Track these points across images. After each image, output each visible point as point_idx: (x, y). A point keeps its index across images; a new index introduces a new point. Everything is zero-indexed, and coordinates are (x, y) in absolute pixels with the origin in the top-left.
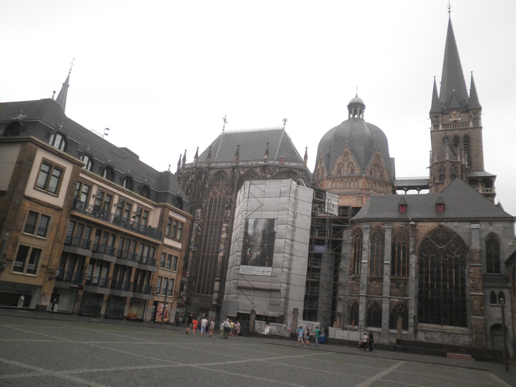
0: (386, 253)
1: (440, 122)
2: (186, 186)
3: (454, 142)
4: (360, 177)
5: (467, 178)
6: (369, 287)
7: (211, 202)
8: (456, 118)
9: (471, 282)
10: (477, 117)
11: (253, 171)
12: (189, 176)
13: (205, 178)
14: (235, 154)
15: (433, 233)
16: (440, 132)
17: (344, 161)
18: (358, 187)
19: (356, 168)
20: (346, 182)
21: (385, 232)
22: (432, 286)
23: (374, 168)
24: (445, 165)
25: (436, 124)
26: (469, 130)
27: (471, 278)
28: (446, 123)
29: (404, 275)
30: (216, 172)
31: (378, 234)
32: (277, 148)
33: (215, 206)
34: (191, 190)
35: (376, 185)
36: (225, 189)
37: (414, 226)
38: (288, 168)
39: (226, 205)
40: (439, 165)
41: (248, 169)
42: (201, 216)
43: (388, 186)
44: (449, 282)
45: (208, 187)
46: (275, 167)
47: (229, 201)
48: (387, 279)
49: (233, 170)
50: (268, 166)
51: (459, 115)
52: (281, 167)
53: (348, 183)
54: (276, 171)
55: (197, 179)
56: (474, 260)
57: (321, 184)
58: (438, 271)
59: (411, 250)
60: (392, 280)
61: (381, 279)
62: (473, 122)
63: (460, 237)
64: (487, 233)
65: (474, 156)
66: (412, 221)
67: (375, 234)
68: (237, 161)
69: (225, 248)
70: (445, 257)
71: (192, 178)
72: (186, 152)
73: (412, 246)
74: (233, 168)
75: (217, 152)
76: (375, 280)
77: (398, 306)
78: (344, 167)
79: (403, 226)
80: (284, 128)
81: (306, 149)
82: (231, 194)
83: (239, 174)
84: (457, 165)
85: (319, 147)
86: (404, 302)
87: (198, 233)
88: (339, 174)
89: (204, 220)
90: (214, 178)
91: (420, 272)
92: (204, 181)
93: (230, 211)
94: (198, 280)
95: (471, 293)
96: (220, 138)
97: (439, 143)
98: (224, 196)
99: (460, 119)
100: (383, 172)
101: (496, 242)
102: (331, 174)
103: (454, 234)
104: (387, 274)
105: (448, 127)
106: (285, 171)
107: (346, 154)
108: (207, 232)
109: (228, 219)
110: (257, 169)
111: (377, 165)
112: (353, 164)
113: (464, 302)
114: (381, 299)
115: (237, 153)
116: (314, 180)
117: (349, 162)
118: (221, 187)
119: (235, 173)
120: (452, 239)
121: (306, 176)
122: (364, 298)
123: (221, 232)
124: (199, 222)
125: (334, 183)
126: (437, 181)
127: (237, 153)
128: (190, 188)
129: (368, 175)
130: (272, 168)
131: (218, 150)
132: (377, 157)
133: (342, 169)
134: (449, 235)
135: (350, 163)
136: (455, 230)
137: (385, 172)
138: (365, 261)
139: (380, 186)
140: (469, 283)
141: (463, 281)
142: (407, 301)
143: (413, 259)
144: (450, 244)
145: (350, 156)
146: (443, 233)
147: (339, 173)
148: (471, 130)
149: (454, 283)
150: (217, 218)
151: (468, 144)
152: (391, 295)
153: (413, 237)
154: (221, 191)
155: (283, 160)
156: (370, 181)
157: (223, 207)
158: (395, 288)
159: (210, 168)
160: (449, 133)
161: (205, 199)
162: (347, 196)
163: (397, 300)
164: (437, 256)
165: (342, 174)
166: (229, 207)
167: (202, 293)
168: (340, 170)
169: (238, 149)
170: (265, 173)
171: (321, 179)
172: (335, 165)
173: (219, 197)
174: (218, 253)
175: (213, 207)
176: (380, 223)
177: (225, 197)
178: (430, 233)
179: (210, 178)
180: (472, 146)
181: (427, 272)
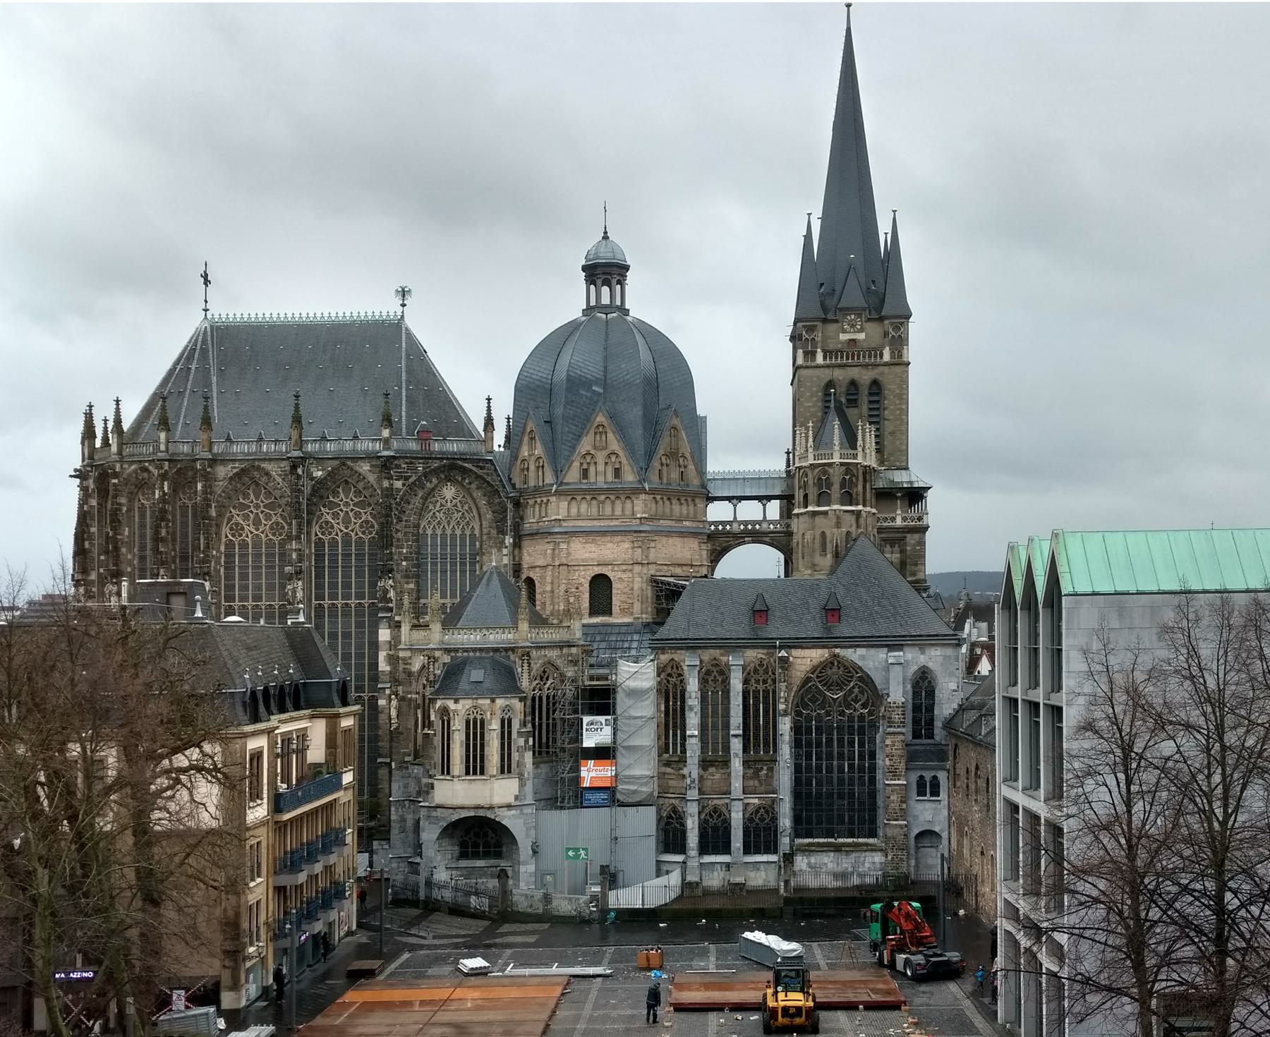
0: (732, 713)
1: (819, 345)
2: (136, 509)
5: (874, 491)
6: (701, 778)
7: (229, 556)
9: (888, 763)
12: (143, 479)
13: (205, 492)
14: (290, 421)
15: (820, 669)
16: (817, 371)
18: (633, 515)
20: (603, 502)
21: (730, 670)
22: (819, 769)
24: (831, 471)
26: (881, 368)
27: (887, 756)
28: (831, 347)
29: (766, 752)
30: (235, 471)
31: (715, 673)
32: (400, 388)
34: (167, 526)
35: (671, 503)
36: (268, 517)
37: (784, 661)
38: (447, 459)
39: (288, 569)
40: (817, 470)
41: (336, 463)
43: (697, 501)
44: (849, 760)
46: (411, 458)
47: (294, 556)
48: (737, 765)
51: (861, 325)
53: (608, 502)
55: (174, 491)
56: (894, 722)
57: (539, 500)
58: (830, 741)
59: (782, 707)
60: (746, 763)
61: (726, 763)
63: (868, 676)
64: (915, 668)
66: (781, 648)
67: (708, 673)
68: (300, 444)
70: (842, 713)
71: (164, 492)
72: (118, 404)
73: (782, 700)
76: (712, 766)
77: (757, 811)
78: (595, 463)
79: (764, 657)
80: (402, 317)
81: (489, 403)
82: (298, 538)
84: (855, 471)
85: (519, 390)
86: (770, 803)
88: (586, 481)
91: (797, 743)
93: (300, 583)
95: (887, 782)
96: (204, 341)
97: (815, 399)
98: (267, 536)
99: (862, 336)
100: (685, 467)
101: (930, 682)
103: (858, 671)
104: (737, 755)
105: (836, 358)
106: (439, 468)
107: (601, 429)
110: (361, 463)
111: (673, 454)
113: (873, 795)
114: (727, 801)
115: (297, 420)
116: (514, 486)
118: (255, 511)
119: (299, 477)
120: (854, 679)
121: (495, 477)
122: (695, 804)
125: (574, 502)
126: (810, 508)
127: (297, 420)
128: (163, 524)
130: (406, 463)
131: (215, 389)
133: (592, 469)
134: (850, 672)
136: (860, 663)
137: (691, 467)
138: (693, 729)
139: (681, 504)
140: (882, 762)
141: (873, 755)
142: (774, 800)
143: (785, 726)
144: (851, 691)
145: (610, 435)
146: (839, 668)
148: (886, 369)
149: (856, 762)
152: (744, 794)
153: (784, 682)
156: (658, 497)
157: (281, 572)
158: (751, 778)
160: (838, 374)
162: (609, 538)
163: (756, 801)
164: (827, 711)
165: (592, 479)
166: (297, 573)
169: (297, 406)
170: (390, 478)
171: (535, 486)
173: (252, 538)
176: (718, 651)
178: (813, 670)
179: (219, 486)
180: (884, 409)
181: (809, 744)
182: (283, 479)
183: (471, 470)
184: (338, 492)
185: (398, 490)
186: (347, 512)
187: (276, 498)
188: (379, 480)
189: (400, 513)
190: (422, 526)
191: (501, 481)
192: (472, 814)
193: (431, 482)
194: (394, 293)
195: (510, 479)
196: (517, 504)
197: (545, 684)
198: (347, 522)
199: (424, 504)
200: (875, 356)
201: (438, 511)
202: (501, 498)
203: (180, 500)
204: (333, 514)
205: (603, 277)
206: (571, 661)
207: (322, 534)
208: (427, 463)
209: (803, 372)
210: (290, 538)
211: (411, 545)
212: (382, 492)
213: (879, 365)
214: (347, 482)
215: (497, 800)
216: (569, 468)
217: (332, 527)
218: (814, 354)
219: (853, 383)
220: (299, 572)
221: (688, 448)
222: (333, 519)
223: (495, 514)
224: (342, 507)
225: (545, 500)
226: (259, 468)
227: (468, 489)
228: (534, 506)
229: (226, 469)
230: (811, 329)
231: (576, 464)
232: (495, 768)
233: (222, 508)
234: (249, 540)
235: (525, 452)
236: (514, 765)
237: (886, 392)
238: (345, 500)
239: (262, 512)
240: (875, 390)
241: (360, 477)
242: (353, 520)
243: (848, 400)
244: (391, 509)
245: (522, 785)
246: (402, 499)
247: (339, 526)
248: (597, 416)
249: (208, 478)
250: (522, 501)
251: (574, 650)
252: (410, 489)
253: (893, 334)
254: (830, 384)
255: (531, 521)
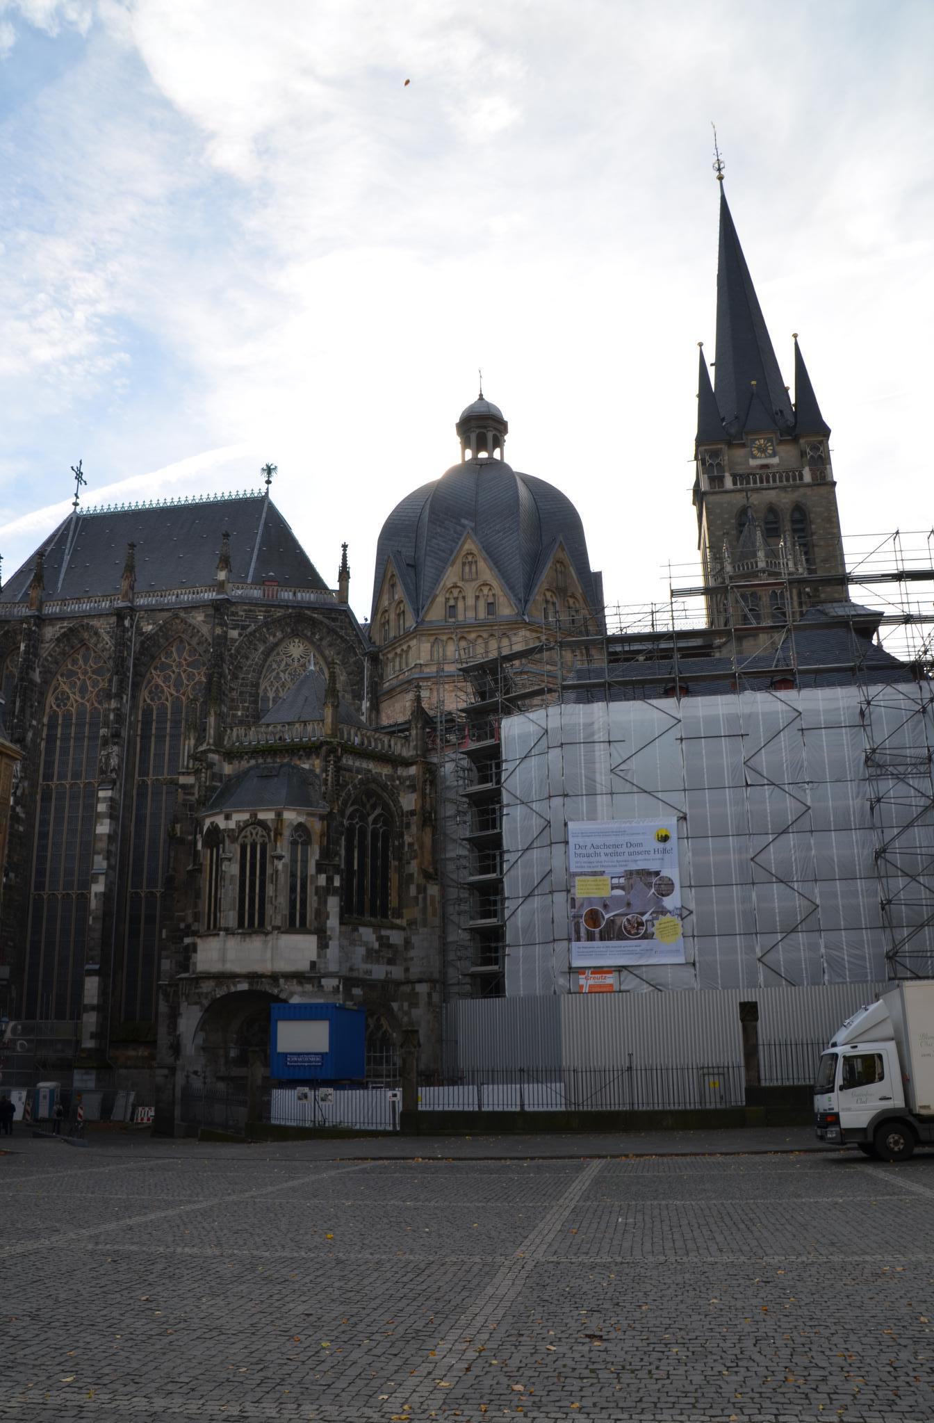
1: (726, 468)
3: (766, 523)
4: (516, 624)
8: (766, 457)
10: (820, 457)
11: (183, 621)
13: (27, 652)
16: (727, 497)
17: (463, 580)
19: (502, 600)
20: (474, 642)
23: (551, 600)
25: (716, 474)
26: (802, 490)
28: (741, 472)
30: (63, 630)
32: (253, 550)
33: (66, 738)
38: (293, 607)
39: (103, 731)
41: (170, 614)
42: (21, 771)
45: (38, 680)
47: (112, 717)
49: (118, 622)
50: (234, 604)
51: (773, 450)
52: (273, 606)
53: (480, 641)
54: (255, 619)
62: (811, 470)
65: (822, 561)
69: (110, 866)
74: (120, 614)
75: (59, 572)
78: (464, 598)
80: (267, 493)
81: (345, 550)
82: (119, 696)
83: (139, 632)
87: (16, 826)
88: (450, 620)
89: (34, 785)
90: (57, 649)
92: (25, 660)
93: (116, 748)
94: (26, 978)
97: (727, 527)
98: (93, 704)
99: (775, 460)
102: (426, 620)
107: (470, 558)
108: (44, 823)
109: (114, 775)
110: (194, 614)
112: (490, 589)
116: (374, 643)
117: (480, 582)
119: (125, 630)
121: (350, 631)
123: (92, 818)
124: (19, 793)
127: (130, 568)
129: (539, 617)
130: (245, 611)
131: (65, 565)
132: (558, 565)
133: (460, 605)
135: (483, 585)
147: (450, 617)
148: (808, 491)
150: (76, 775)
151: (802, 530)
154: (83, 690)
155: (276, 584)
157: (94, 737)
159: (44, 620)
161: (32, 716)
165: (461, 618)
167: (41, 1018)
168: (453, 607)
171: (395, 637)
172: (437, 593)
174: (86, 884)
175: (58, 743)
177: (96, 708)
179: (46, 649)
180: (812, 534)
182: (111, 637)
183: (322, 622)
184: (172, 652)
185: (234, 640)
186: (179, 674)
187: (105, 662)
188: (213, 628)
189: (236, 668)
190: (262, 687)
191: (357, 635)
192: (244, 986)
193: (274, 636)
194: (260, 471)
195: (370, 638)
196: (375, 659)
197: (369, 815)
198: (178, 684)
199: (265, 660)
200: (794, 479)
201: (284, 672)
202: (356, 655)
203: (7, 668)
204: (165, 676)
205: (478, 431)
206: (409, 787)
207: (151, 700)
208: (269, 612)
209: (711, 498)
210: (109, 696)
211: (248, 708)
212: (213, 639)
213: (798, 487)
214: (182, 641)
215: (283, 966)
216: (432, 602)
217: (162, 692)
218: (721, 479)
219: (772, 509)
220: (117, 735)
221: (580, 589)
222: (164, 682)
223: (351, 677)
224: (174, 668)
225: (405, 647)
226: (88, 628)
227: (319, 646)
228: (394, 659)
229: (55, 629)
230: (715, 454)
231: (440, 599)
232: (279, 917)
233: (48, 674)
234: (73, 710)
235: (385, 603)
236: (310, 915)
237: (812, 515)
238: (177, 660)
239: (90, 678)
240: (797, 516)
241: (195, 631)
242: (185, 681)
243: (768, 530)
244: (223, 660)
245: (323, 945)
246: (238, 651)
247: (169, 691)
248: (464, 542)
249: (34, 640)
250: (381, 657)
251: (413, 770)
252: (250, 642)
253: (811, 454)
254: (743, 511)
255: (392, 674)
